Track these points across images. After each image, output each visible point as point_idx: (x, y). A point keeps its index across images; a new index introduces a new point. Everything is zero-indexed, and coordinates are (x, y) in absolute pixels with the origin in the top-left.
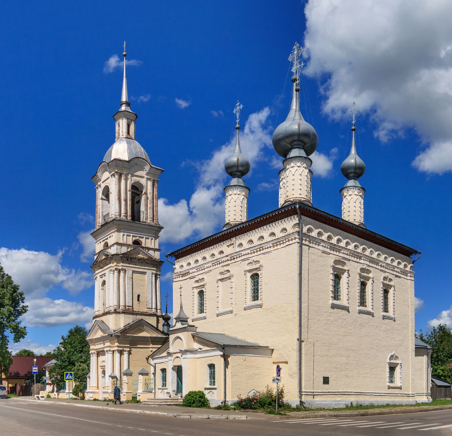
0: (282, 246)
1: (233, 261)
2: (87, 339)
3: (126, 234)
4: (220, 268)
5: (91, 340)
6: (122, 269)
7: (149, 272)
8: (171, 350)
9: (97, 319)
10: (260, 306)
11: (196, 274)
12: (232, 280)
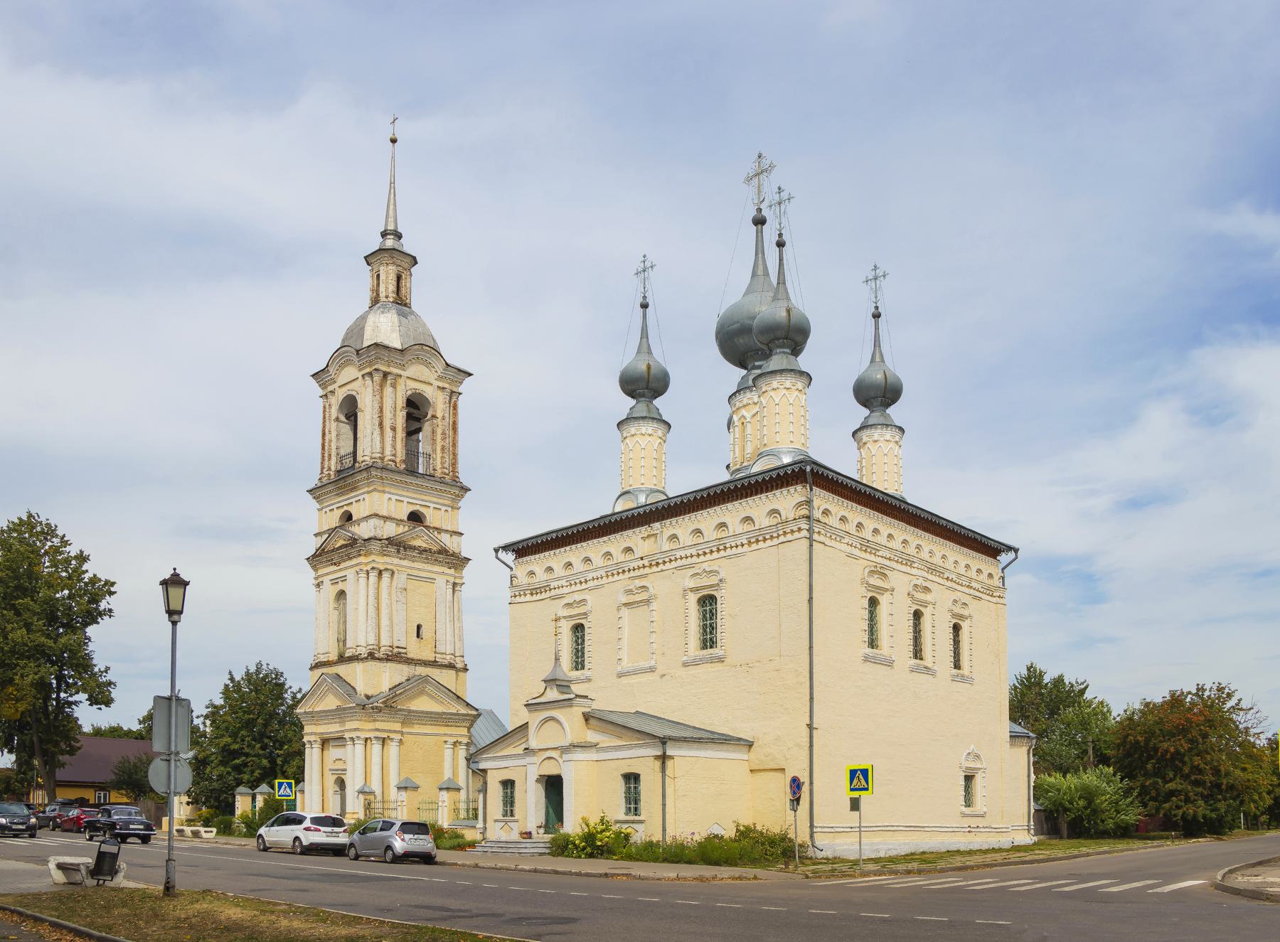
0: (769, 543)
1: (655, 569)
2: (298, 711)
5: (312, 714)
6: (386, 569)
8: (534, 743)
9: (324, 670)
10: (721, 660)
11: (566, 590)
12: (654, 605)
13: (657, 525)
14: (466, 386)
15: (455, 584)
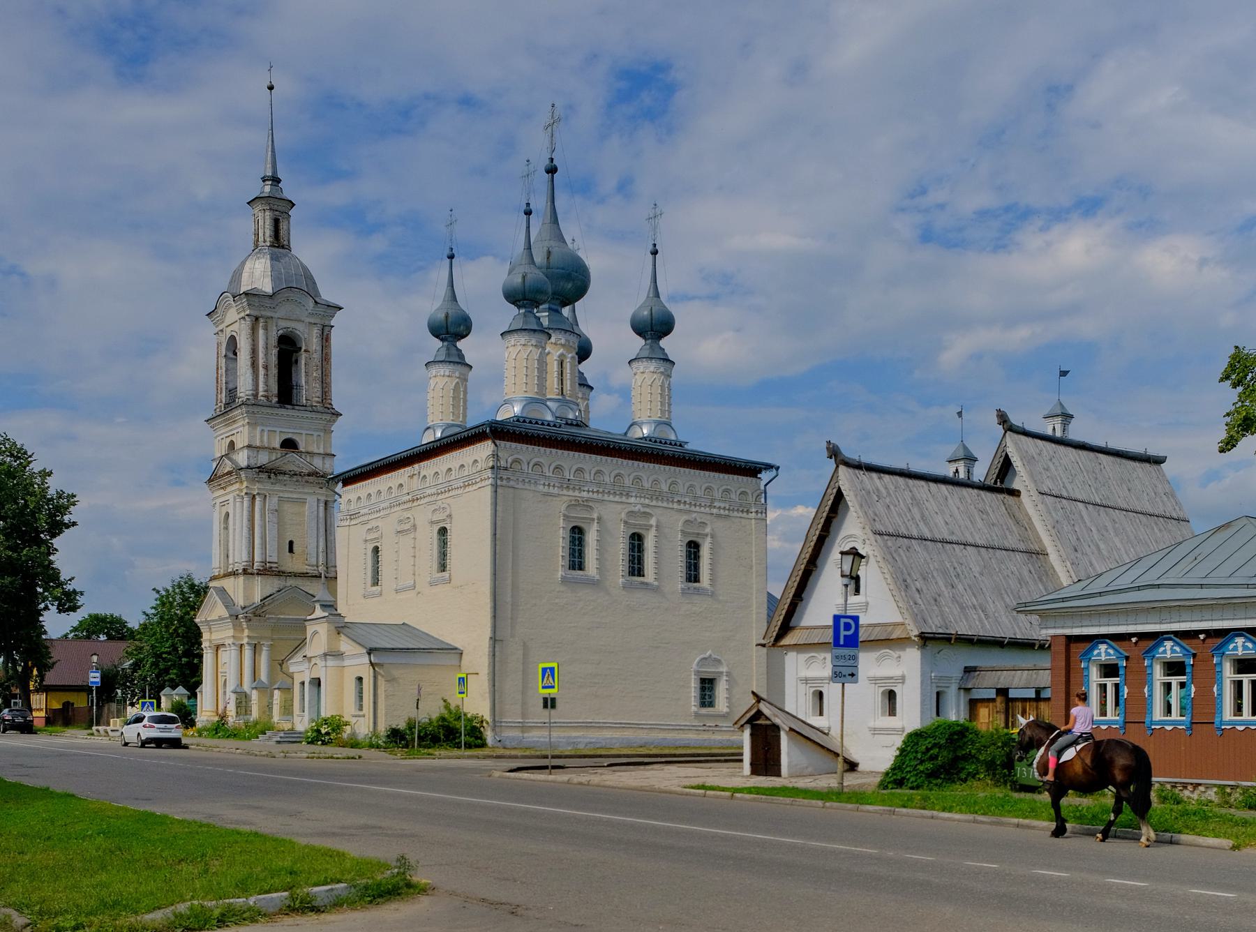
3: (266, 429)
4: (398, 513)
7: (311, 500)
13: (416, 466)
14: (337, 320)
15: (326, 503)
